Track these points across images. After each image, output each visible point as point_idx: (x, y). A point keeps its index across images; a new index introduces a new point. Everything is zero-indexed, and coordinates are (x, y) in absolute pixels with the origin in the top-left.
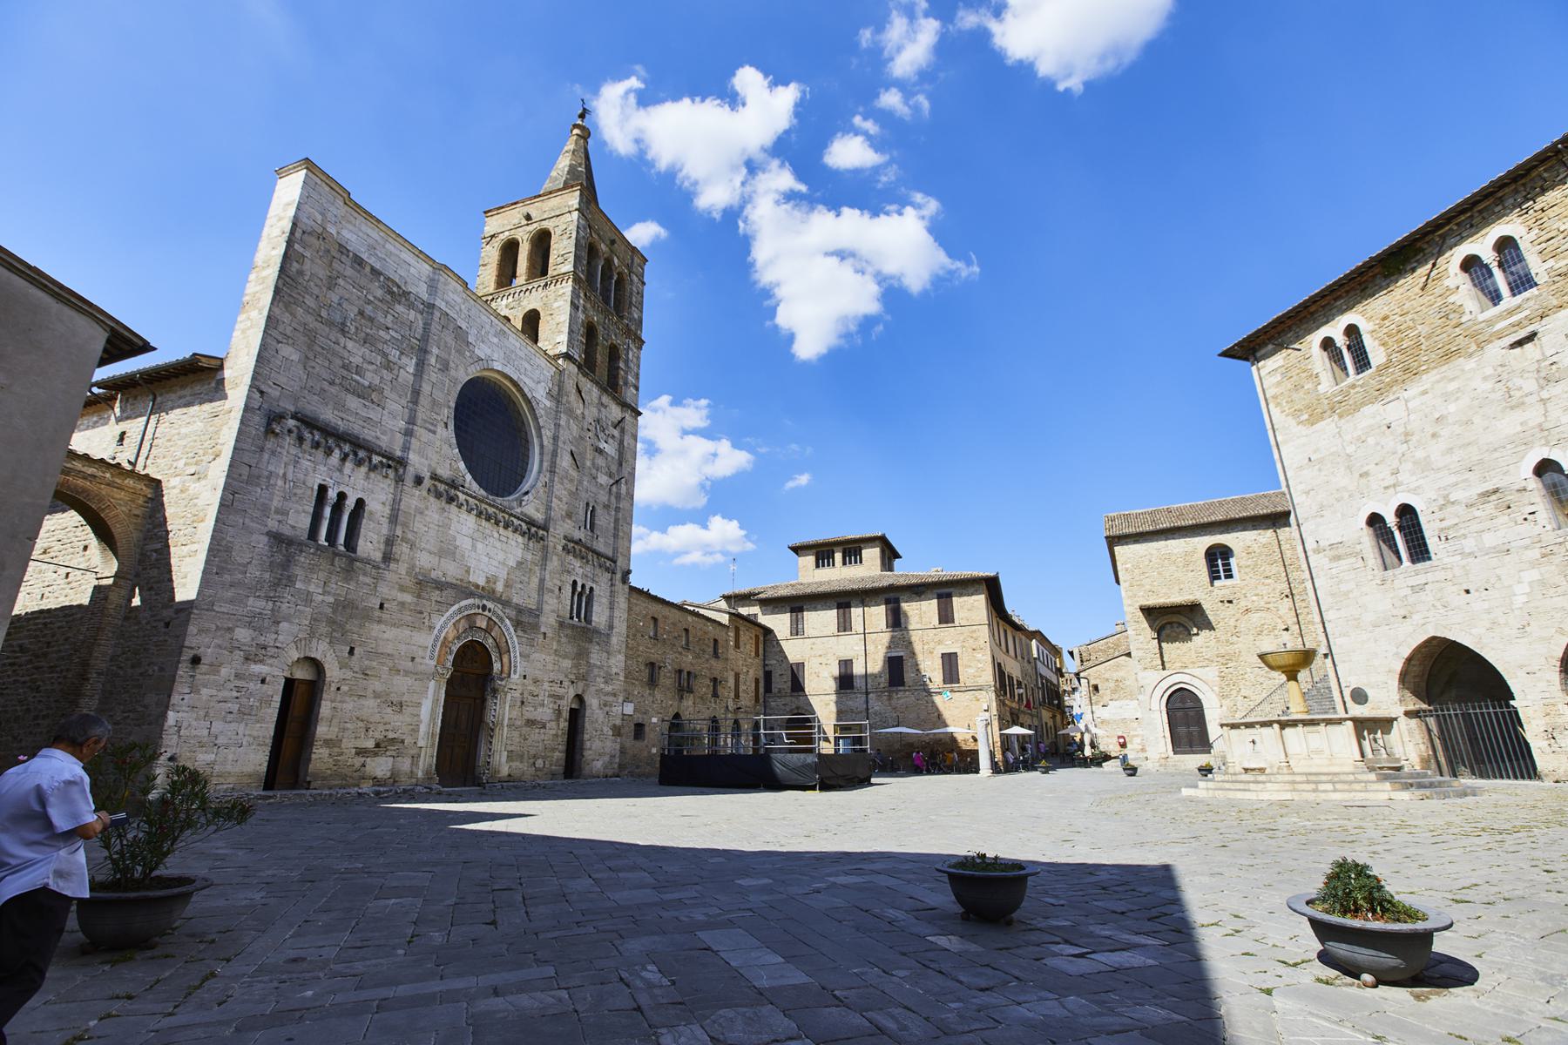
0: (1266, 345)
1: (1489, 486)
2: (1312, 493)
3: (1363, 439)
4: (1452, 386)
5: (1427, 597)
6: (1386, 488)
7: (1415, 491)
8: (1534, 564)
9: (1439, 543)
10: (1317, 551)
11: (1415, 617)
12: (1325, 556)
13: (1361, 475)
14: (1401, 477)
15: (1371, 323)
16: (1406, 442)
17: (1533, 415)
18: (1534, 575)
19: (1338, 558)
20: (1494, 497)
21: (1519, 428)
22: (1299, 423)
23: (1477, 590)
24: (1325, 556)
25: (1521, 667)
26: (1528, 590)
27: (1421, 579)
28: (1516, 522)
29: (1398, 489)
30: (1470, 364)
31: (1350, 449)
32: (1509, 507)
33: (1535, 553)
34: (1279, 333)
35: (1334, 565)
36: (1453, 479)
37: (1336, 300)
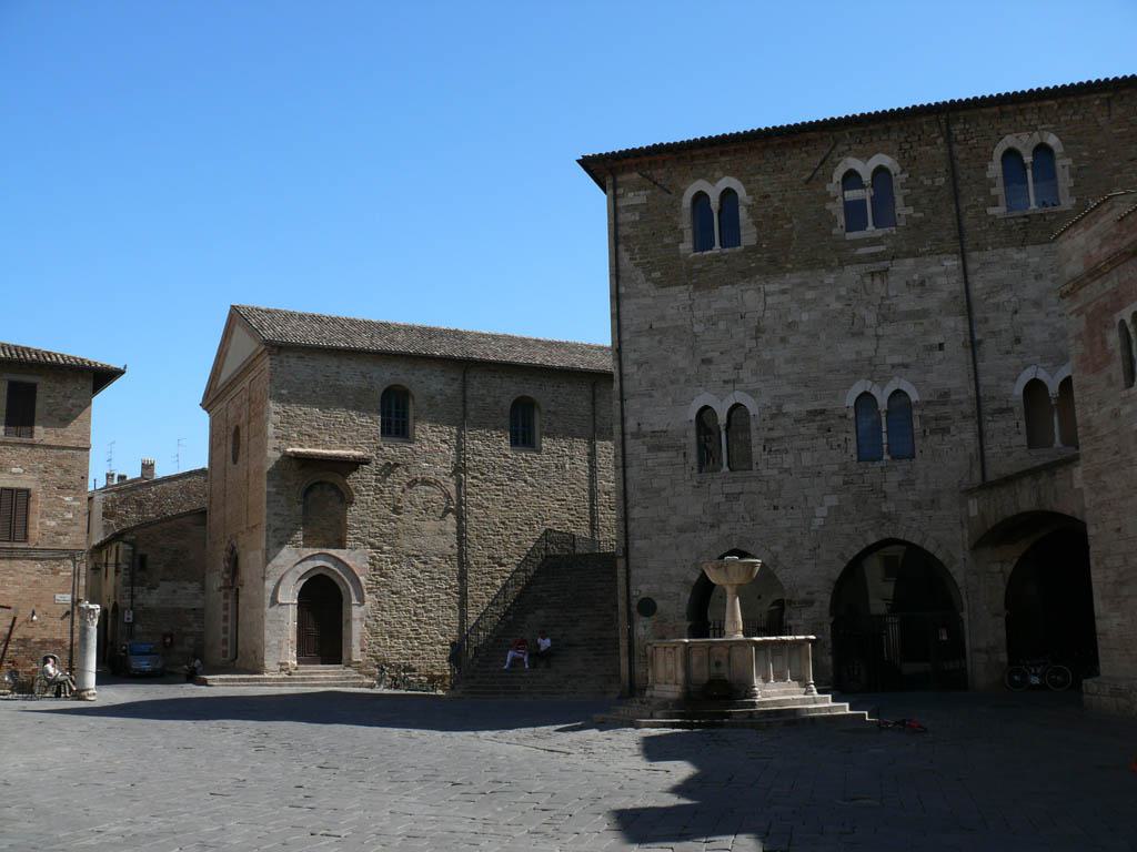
0: (631, 171)
1: (816, 405)
3: (715, 319)
4: (810, 295)
6: (725, 382)
7: (753, 393)
8: (835, 490)
10: (636, 435)
11: (724, 528)
12: (644, 443)
13: (703, 360)
14: (744, 374)
15: (751, 197)
16: (756, 338)
17: (866, 347)
18: (832, 500)
19: (659, 448)
20: (819, 418)
21: (854, 356)
22: (647, 280)
23: (784, 508)
26: (825, 514)
27: (736, 488)
29: (737, 386)
30: (830, 279)
31: (698, 328)
33: (838, 480)
34: (650, 163)
36: (788, 389)
37: (722, 153)
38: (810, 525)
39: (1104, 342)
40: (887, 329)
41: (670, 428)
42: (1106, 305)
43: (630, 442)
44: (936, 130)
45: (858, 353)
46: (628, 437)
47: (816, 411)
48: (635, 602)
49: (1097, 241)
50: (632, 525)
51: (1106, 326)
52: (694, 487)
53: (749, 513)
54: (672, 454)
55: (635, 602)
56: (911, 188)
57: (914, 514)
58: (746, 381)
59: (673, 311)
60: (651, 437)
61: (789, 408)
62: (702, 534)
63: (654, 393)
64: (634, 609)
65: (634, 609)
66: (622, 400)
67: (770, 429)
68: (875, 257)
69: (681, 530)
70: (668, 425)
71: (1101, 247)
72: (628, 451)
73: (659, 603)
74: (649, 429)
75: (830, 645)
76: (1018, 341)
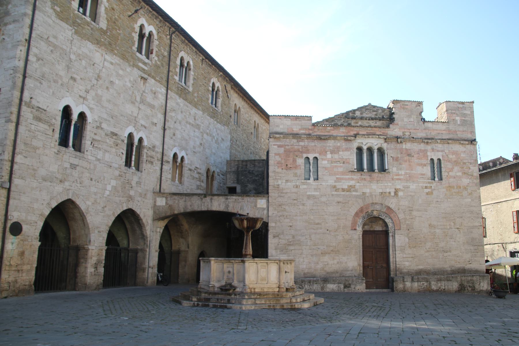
1: (115, 130)
2: (41, 62)
3: (81, 57)
5: (75, 173)
6: (80, 96)
7: (91, 109)
9: (90, 146)
10: (29, 105)
11: (67, 184)
16: (97, 80)
18: (113, 183)
19: (38, 119)
21: (130, 113)
23: (95, 181)
24: (31, 112)
25: (98, 228)
28: (117, 154)
31: (73, 57)
32: (117, 146)
33: (117, 173)
35: (35, 123)
38: (104, 194)
39: (294, 161)
40: (142, 107)
41: (47, 110)
42: (299, 149)
43: (24, 108)
44: (168, 32)
45: (132, 112)
46: (23, 103)
47: (114, 133)
48: (9, 225)
49: (300, 127)
50: (15, 167)
51: (297, 156)
52: (55, 152)
53: (79, 178)
54: (46, 127)
55: (9, 225)
56: (159, 50)
57: (139, 199)
58: (89, 101)
59: (61, 37)
60: (37, 110)
61: (104, 126)
62: (55, 184)
63: (43, 82)
64: (8, 229)
65: (8, 229)
66: (24, 77)
67: (95, 134)
68: (143, 70)
69: (44, 180)
70: (48, 107)
71: (300, 130)
72: (22, 113)
73: (25, 227)
74: (37, 104)
75: (104, 262)
76: (174, 135)
